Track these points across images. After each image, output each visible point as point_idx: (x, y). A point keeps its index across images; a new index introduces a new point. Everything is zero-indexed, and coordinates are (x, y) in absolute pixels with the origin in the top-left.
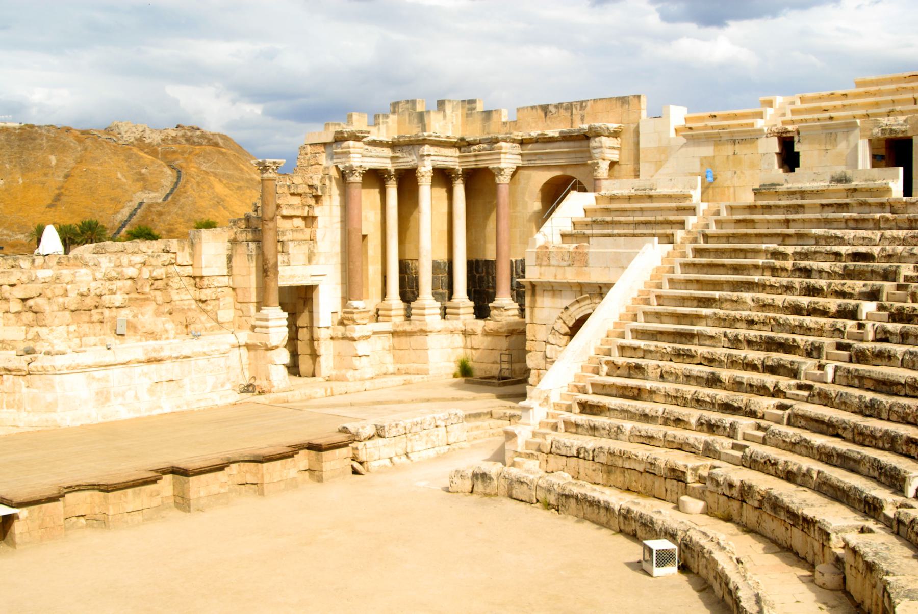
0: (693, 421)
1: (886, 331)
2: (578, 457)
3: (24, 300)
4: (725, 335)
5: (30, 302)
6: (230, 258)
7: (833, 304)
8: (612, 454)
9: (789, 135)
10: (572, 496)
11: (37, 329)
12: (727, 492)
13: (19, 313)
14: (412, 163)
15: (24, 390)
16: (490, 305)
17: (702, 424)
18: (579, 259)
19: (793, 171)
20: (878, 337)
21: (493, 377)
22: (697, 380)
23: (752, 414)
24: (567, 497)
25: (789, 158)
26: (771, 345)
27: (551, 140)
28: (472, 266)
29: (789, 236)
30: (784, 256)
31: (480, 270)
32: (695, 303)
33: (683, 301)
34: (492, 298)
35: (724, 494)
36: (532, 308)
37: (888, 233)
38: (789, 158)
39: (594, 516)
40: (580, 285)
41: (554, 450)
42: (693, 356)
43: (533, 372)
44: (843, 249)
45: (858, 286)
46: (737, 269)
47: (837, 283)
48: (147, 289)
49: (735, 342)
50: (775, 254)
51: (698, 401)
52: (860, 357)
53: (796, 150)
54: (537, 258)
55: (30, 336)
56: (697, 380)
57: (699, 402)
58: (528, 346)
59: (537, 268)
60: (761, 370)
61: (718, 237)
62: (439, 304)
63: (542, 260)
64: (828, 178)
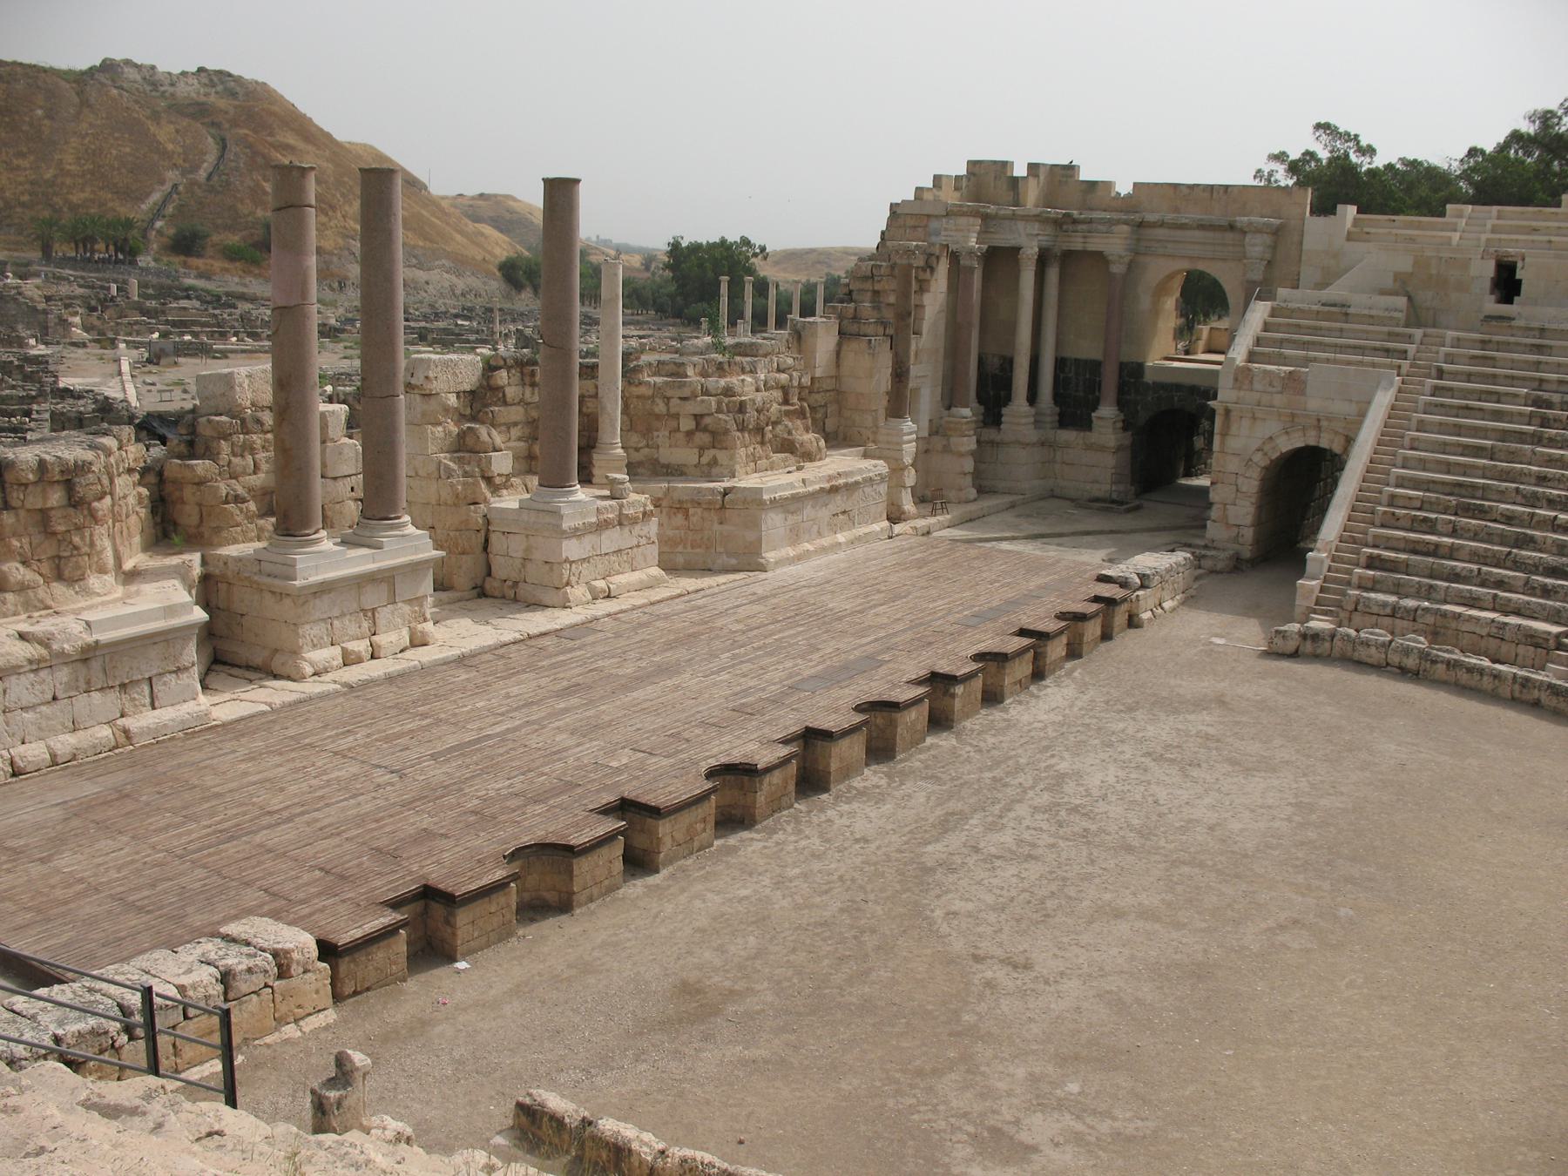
2: (1393, 616)
3: (698, 417)
5: (707, 420)
6: (838, 353)
11: (712, 452)
13: (689, 434)
15: (716, 527)
17: (1534, 588)
21: (1097, 500)
22: (1503, 539)
24: (1434, 662)
25: (1507, 283)
27: (1182, 227)
28: (1060, 363)
29: (1547, 381)
30: (1550, 405)
32: (1460, 450)
33: (1444, 448)
36: (1224, 435)
38: (1507, 283)
39: (1473, 683)
46: (1498, 415)
48: (795, 400)
49: (1532, 500)
51: (1515, 562)
53: (1518, 277)
54: (1236, 380)
55: (705, 460)
56: (1503, 539)
57: (1517, 565)
61: (1455, 376)
62: (1033, 411)
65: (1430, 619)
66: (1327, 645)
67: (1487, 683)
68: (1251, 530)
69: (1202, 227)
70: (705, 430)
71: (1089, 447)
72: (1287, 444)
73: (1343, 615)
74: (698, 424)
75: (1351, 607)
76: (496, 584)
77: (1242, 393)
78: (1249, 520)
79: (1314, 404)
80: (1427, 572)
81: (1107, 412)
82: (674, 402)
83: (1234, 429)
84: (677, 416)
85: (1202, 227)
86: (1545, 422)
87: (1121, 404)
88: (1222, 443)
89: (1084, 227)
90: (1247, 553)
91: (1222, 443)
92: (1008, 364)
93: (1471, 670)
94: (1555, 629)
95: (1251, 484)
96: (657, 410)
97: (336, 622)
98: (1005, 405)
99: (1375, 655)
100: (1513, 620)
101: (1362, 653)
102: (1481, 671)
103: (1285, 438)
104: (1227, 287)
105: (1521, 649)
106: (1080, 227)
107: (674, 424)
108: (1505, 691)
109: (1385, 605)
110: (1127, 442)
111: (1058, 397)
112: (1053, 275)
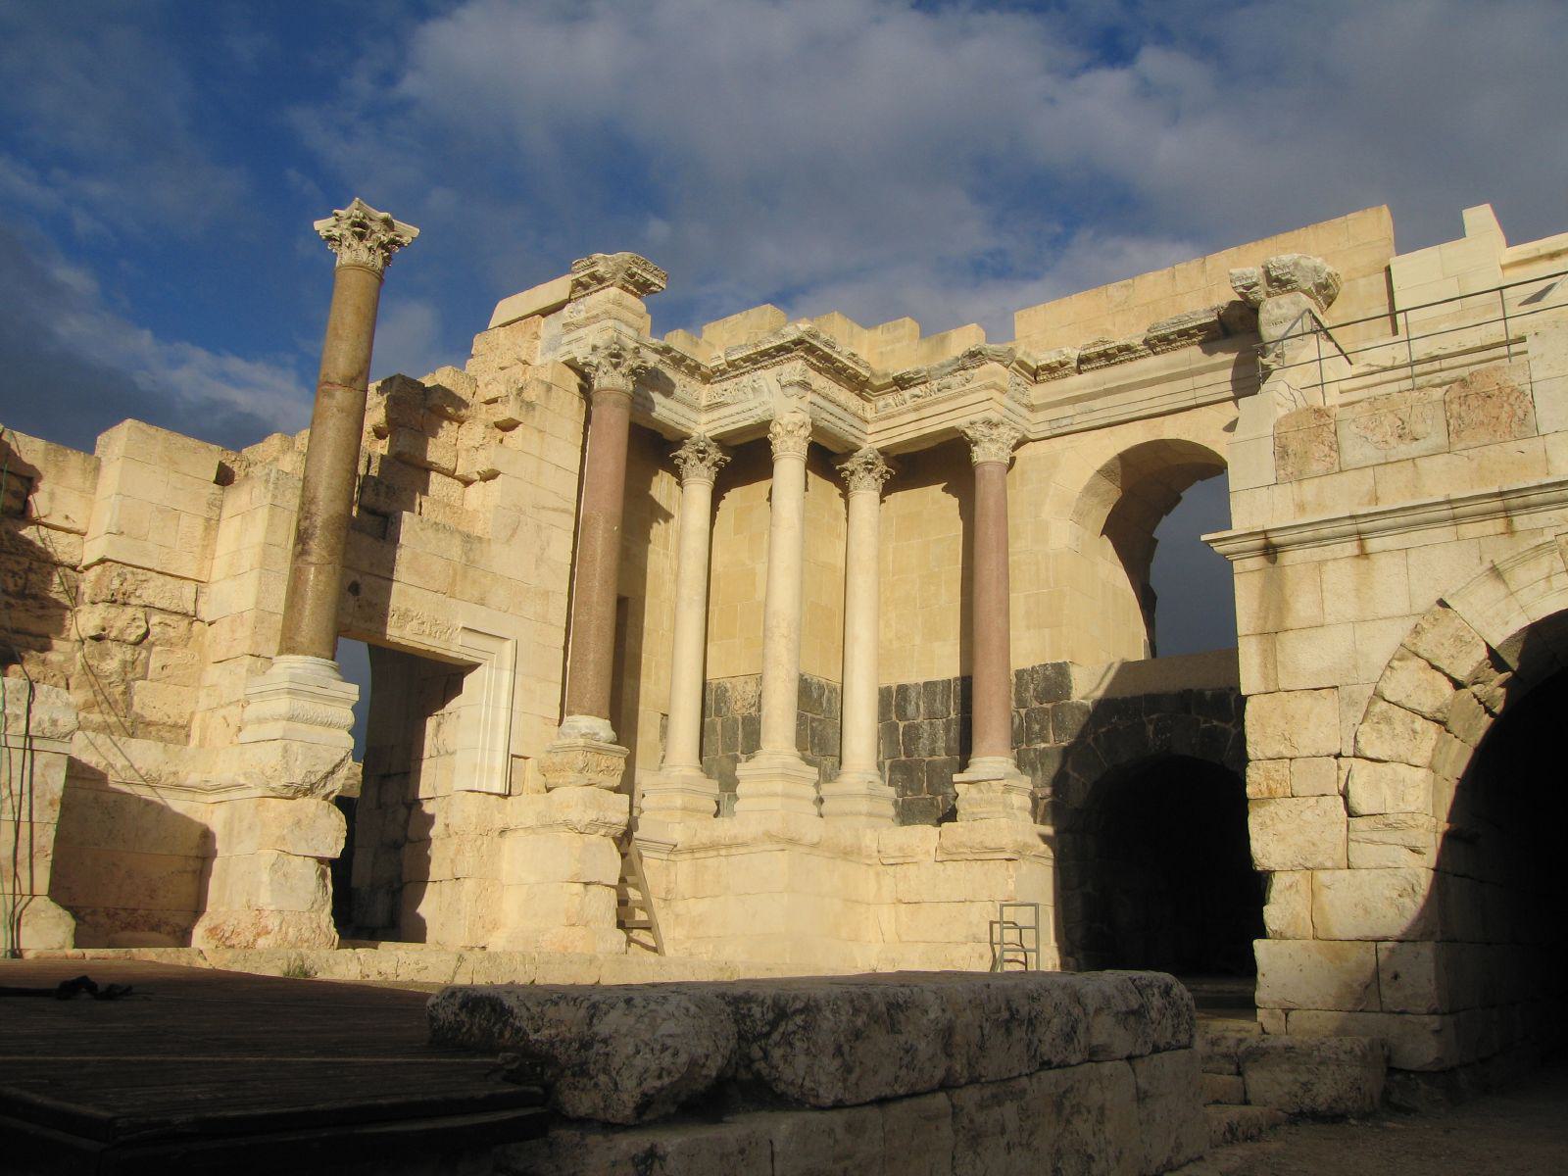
14: (759, 411)
16: (956, 777)
31: (911, 709)
36: (1271, 635)
40: (1507, 505)
43: (1279, 883)
54: (1282, 453)
58: (1256, 781)
59: (1288, 491)
71: (948, 855)
77: (1309, 489)
85: (1157, 343)
88: (1270, 661)
91: (1270, 661)
103: (1491, 590)
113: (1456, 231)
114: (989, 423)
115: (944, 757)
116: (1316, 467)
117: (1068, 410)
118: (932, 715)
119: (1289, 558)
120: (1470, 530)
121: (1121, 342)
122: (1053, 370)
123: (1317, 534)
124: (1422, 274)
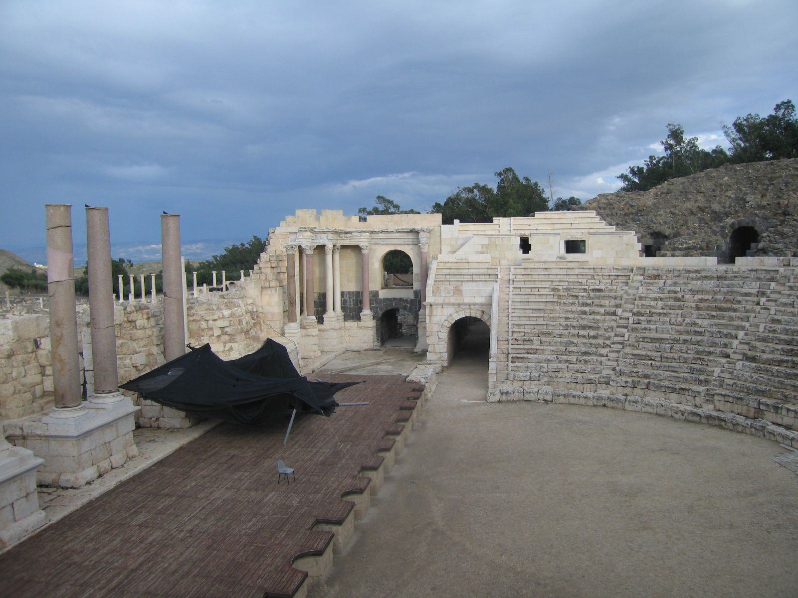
0: (575, 360)
1: (639, 320)
2: (530, 380)
3: (222, 328)
4: (560, 324)
5: (226, 329)
7: (602, 310)
8: (551, 377)
9: (526, 236)
10: (562, 395)
12: (624, 385)
13: (219, 337)
18: (458, 291)
19: (528, 253)
20: (635, 322)
23: (602, 355)
25: (525, 246)
26: (584, 328)
27: (392, 232)
28: (342, 294)
30: (558, 290)
31: (345, 296)
34: (360, 310)
35: (621, 386)
36: (430, 316)
37: (603, 281)
38: (525, 246)
40: (459, 305)
41: (516, 378)
42: (551, 334)
44: (587, 287)
45: (607, 302)
47: (596, 301)
50: (553, 290)
51: (569, 352)
52: (633, 330)
54: (433, 292)
55: (227, 349)
59: (434, 298)
60: (588, 338)
63: (436, 293)
64: (556, 257)
65: (546, 379)
66: (512, 395)
67: (582, 401)
68: (446, 354)
69: (399, 232)
70: (226, 334)
71: (360, 328)
72: (457, 317)
73: (509, 382)
74: (222, 331)
75: (512, 379)
76: (146, 421)
78: (445, 350)
79: (467, 300)
80: (537, 361)
81: (367, 313)
82: (211, 322)
83: (435, 313)
84: (212, 329)
85: (399, 232)
86: (559, 297)
87: (371, 309)
89: (349, 235)
90: (446, 364)
92: (323, 296)
93: (574, 397)
94: (597, 376)
95: (444, 335)
96: (202, 327)
97: (93, 452)
98: (324, 313)
99: (532, 397)
100: (580, 376)
101: (527, 397)
102: (579, 397)
103: (456, 314)
104: (411, 257)
105: (585, 386)
106: (348, 235)
107: (211, 333)
108: (590, 403)
109: (526, 376)
110: (375, 325)
111: (343, 308)
112: (337, 256)
113: (452, 223)
114: (367, 247)
115: (352, 306)
116: (437, 295)
117: (379, 241)
118: (350, 298)
119: (433, 306)
120: (455, 306)
121: (392, 230)
122: (377, 232)
123: (437, 305)
124: (446, 228)
